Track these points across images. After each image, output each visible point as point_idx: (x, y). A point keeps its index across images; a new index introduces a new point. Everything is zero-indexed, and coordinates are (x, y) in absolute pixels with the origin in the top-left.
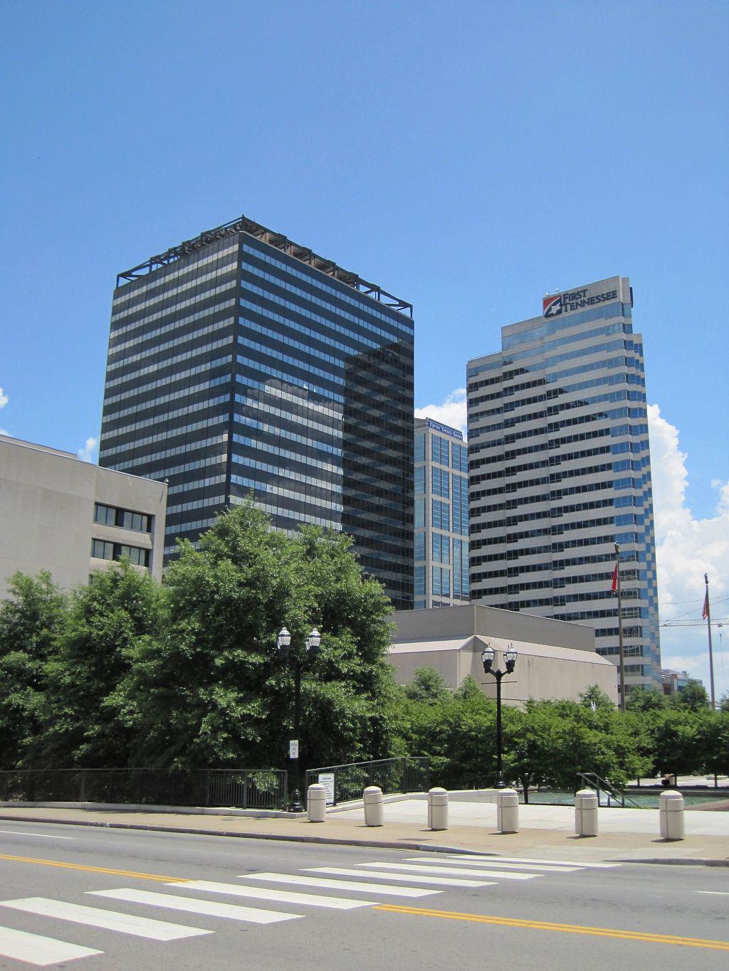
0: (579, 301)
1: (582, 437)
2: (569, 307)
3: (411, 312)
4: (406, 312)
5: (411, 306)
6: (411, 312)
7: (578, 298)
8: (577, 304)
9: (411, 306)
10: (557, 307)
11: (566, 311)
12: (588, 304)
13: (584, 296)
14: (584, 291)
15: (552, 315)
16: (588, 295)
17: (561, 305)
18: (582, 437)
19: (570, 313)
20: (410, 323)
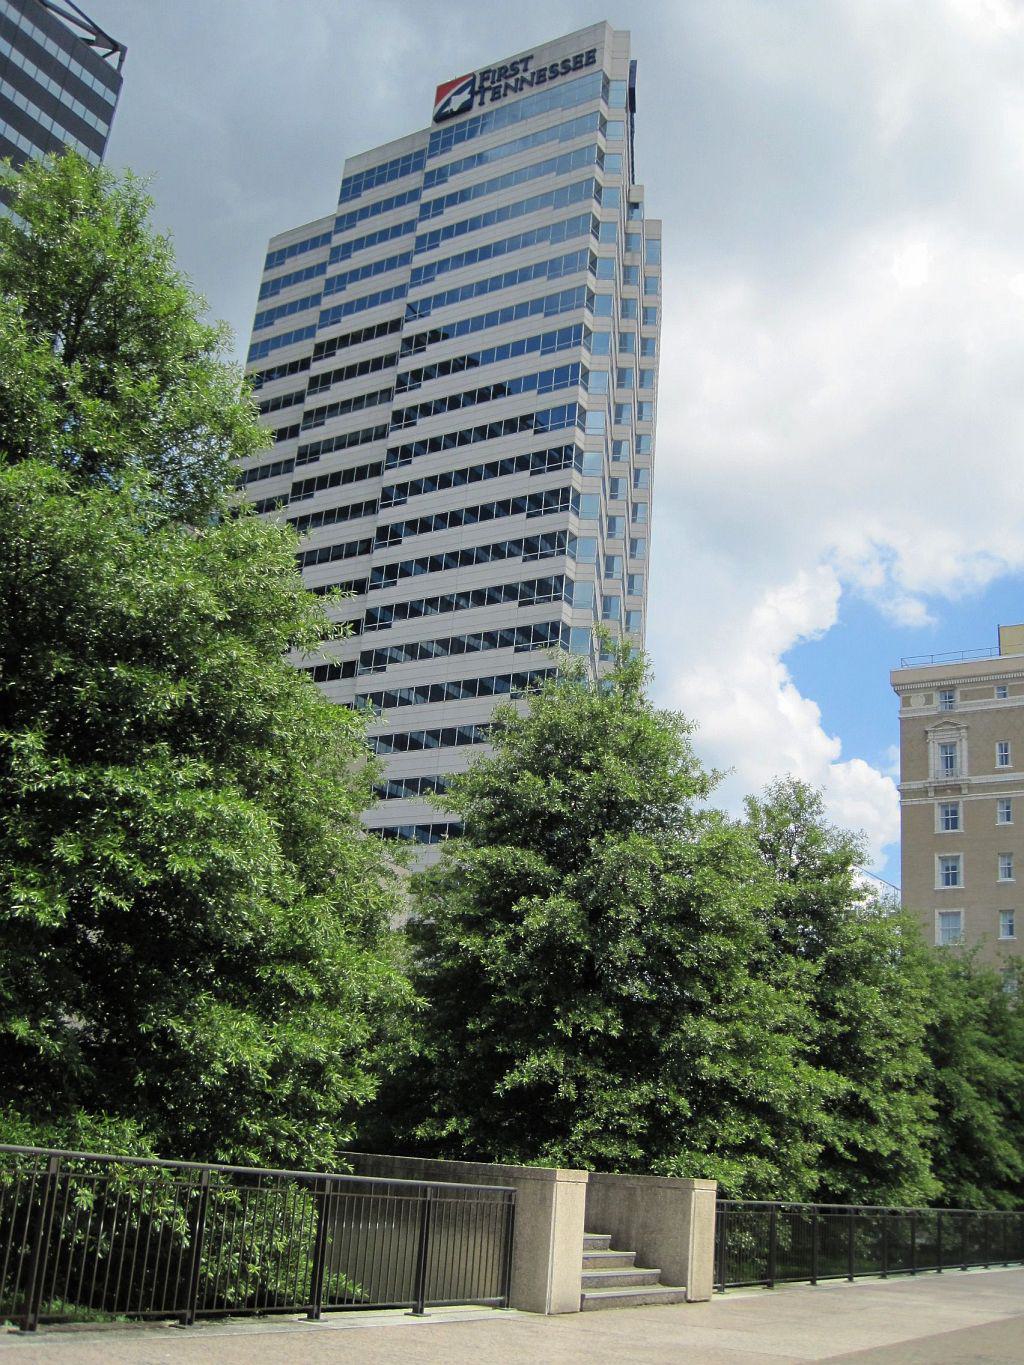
0: (512, 82)
1: (473, 475)
2: (488, 95)
3: (121, 60)
4: (113, 60)
5: (124, 50)
6: (121, 60)
7: (511, 76)
8: (507, 86)
9: (124, 50)
10: (465, 96)
11: (482, 103)
12: (531, 84)
13: (526, 70)
14: (526, 60)
15: (453, 114)
16: (533, 66)
17: (473, 93)
18: (473, 475)
19: (489, 107)
20: (114, 81)
